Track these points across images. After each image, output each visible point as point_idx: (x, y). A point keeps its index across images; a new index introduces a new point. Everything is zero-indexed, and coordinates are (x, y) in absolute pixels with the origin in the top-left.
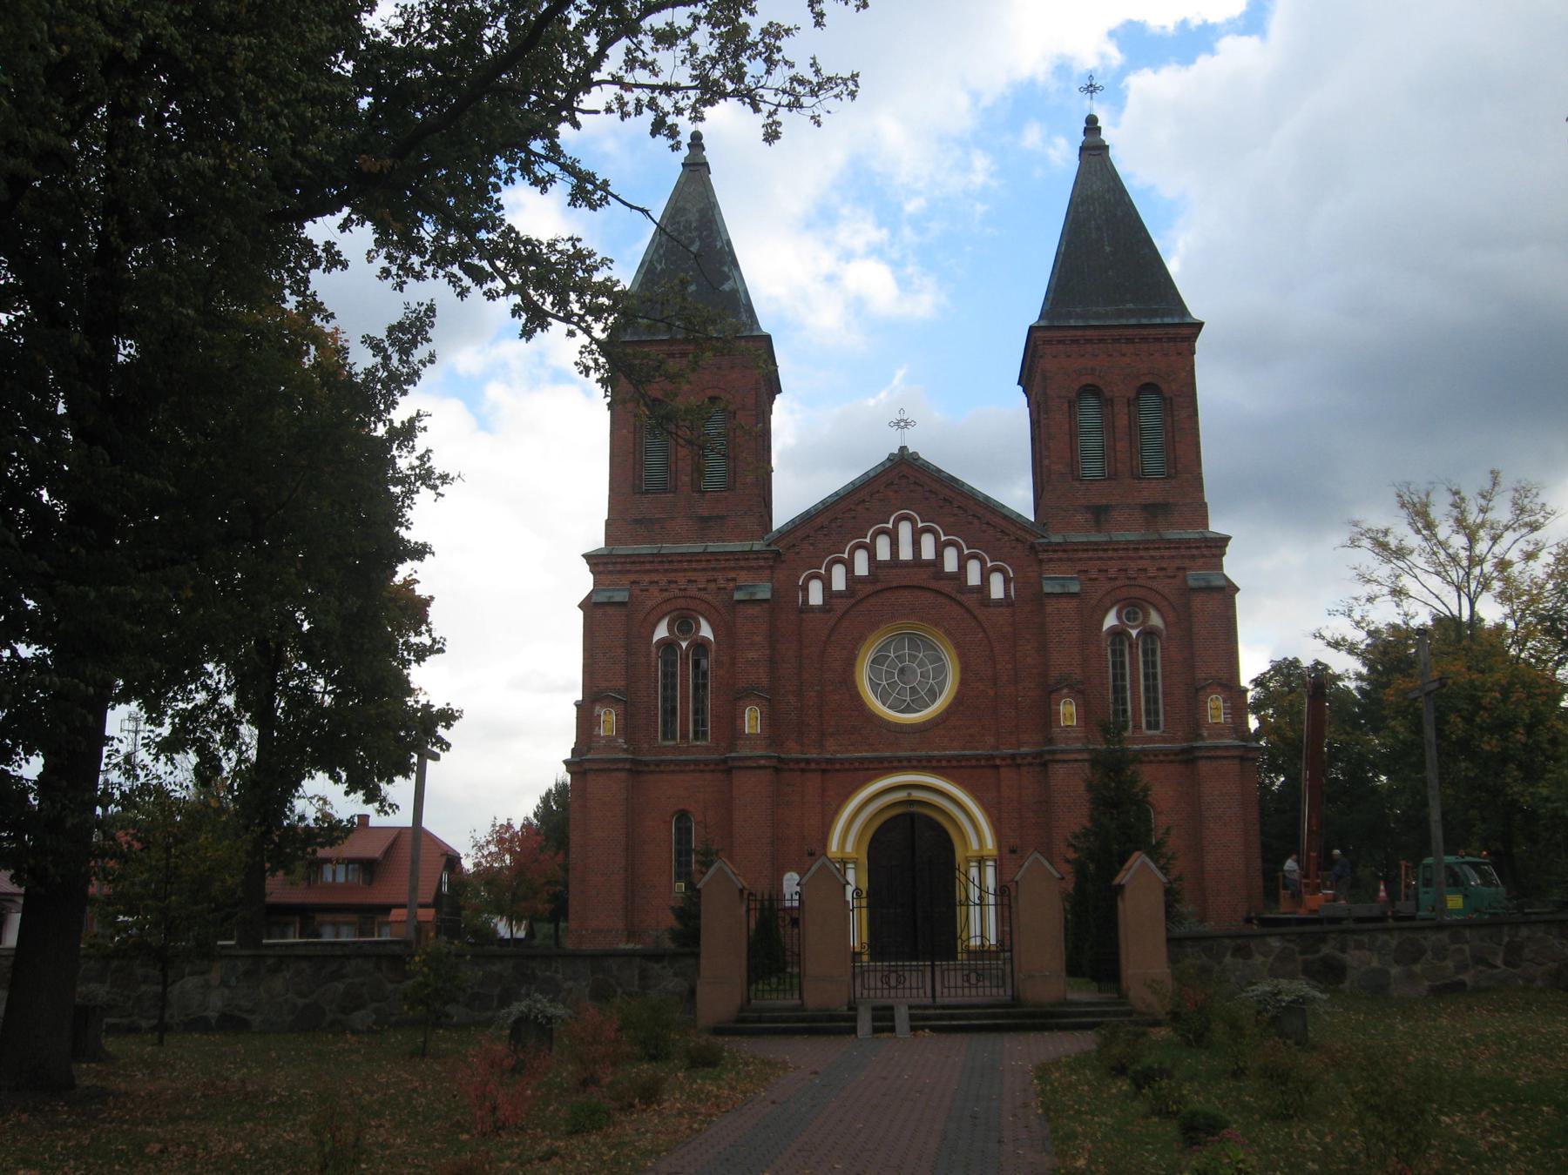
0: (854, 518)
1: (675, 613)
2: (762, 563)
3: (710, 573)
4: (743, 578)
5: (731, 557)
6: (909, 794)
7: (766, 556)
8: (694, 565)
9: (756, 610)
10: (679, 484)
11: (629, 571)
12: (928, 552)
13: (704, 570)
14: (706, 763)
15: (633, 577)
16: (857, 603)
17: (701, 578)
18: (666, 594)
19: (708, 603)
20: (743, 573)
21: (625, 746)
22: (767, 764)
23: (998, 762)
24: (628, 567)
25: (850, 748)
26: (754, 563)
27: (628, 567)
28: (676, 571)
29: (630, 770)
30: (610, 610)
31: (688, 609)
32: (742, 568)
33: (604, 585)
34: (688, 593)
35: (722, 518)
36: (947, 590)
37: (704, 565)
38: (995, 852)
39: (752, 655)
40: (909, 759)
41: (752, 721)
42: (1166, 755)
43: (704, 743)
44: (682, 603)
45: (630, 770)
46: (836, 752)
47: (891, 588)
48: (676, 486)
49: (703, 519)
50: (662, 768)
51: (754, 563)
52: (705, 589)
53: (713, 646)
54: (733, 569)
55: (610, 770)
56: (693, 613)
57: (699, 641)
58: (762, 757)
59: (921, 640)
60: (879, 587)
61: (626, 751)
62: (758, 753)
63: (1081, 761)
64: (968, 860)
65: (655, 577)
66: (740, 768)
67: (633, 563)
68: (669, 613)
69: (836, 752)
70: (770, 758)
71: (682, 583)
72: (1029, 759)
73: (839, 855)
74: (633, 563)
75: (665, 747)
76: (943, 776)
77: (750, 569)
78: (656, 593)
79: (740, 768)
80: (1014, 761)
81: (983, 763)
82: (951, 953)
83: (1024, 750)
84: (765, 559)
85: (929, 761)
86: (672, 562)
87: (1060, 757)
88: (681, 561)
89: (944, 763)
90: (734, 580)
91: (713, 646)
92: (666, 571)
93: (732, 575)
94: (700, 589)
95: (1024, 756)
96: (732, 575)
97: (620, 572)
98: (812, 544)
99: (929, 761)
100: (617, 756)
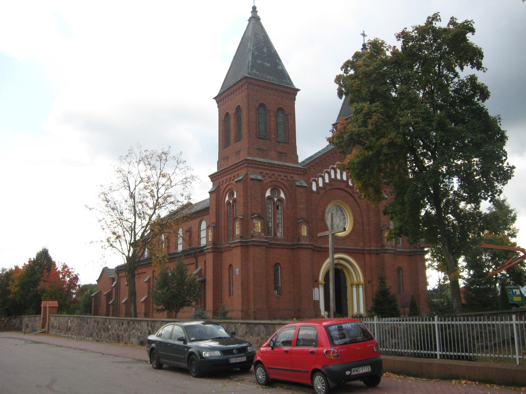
0: (326, 162)
1: (272, 187)
2: (302, 173)
3: (285, 174)
4: (296, 177)
5: (293, 169)
6: (338, 261)
7: (304, 170)
8: (281, 170)
9: (301, 190)
10: (271, 138)
11: (259, 168)
12: (345, 178)
13: (284, 172)
14: (286, 245)
15: (260, 171)
16: (326, 192)
17: (283, 175)
18: (271, 179)
19: (284, 185)
20: (295, 175)
21: (265, 237)
22: (311, 247)
23: (365, 252)
24: (260, 166)
25: (325, 243)
26: (299, 172)
27: (260, 166)
28: (275, 171)
29: (241, 246)
30: (255, 182)
31: (278, 186)
32: (296, 174)
33: (251, 172)
34: (278, 180)
35: (285, 153)
36: (350, 191)
37: (284, 170)
38: (363, 282)
39: (301, 206)
40: (342, 249)
41: (304, 231)
42: (344, 250)
43: (271, 237)
44: (275, 183)
45: (241, 246)
46: (321, 244)
47: (335, 188)
48: (270, 138)
49: (280, 153)
50: (272, 246)
51: (299, 172)
52: (283, 179)
53: (285, 202)
54: (293, 173)
55: (261, 245)
56: (278, 187)
57: (280, 199)
58: (309, 245)
59: (339, 208)
60: (332, 187)
61: (265, 238)
62: (307, 243)
63: (392, 253)
64: (352, 285)
65: (268, 172)
66: (303, 248)
67: (261, 165)
68: (271, 186)
69: (321, 244)
70: (312, 245)
71: (276, 175)
72: (374, 252)
73: (357, 283)
74: (261, 165)
75: (402, 244)
76: (351, 256)
77: (298, 174)
78: (268, 178)
79: (303, 248)
80: (370, 252)
81: (361, 252)
82: (346, 315)
83: (372, 248)
84: (303, 171)
85: (347, 250)
86: (283, 168)
87: (387, 251)
88: (277, 167)
89: (351, 251)
90: (292, 177)
91: (285, 202)
92: (272, 170)
93: (292, 175)
94: (282, 179)
95: (373, 250)
96: (292, 175)
97: (256, 168)
98: (314, 169)
99: (347, 250)
100: (262, 240)
